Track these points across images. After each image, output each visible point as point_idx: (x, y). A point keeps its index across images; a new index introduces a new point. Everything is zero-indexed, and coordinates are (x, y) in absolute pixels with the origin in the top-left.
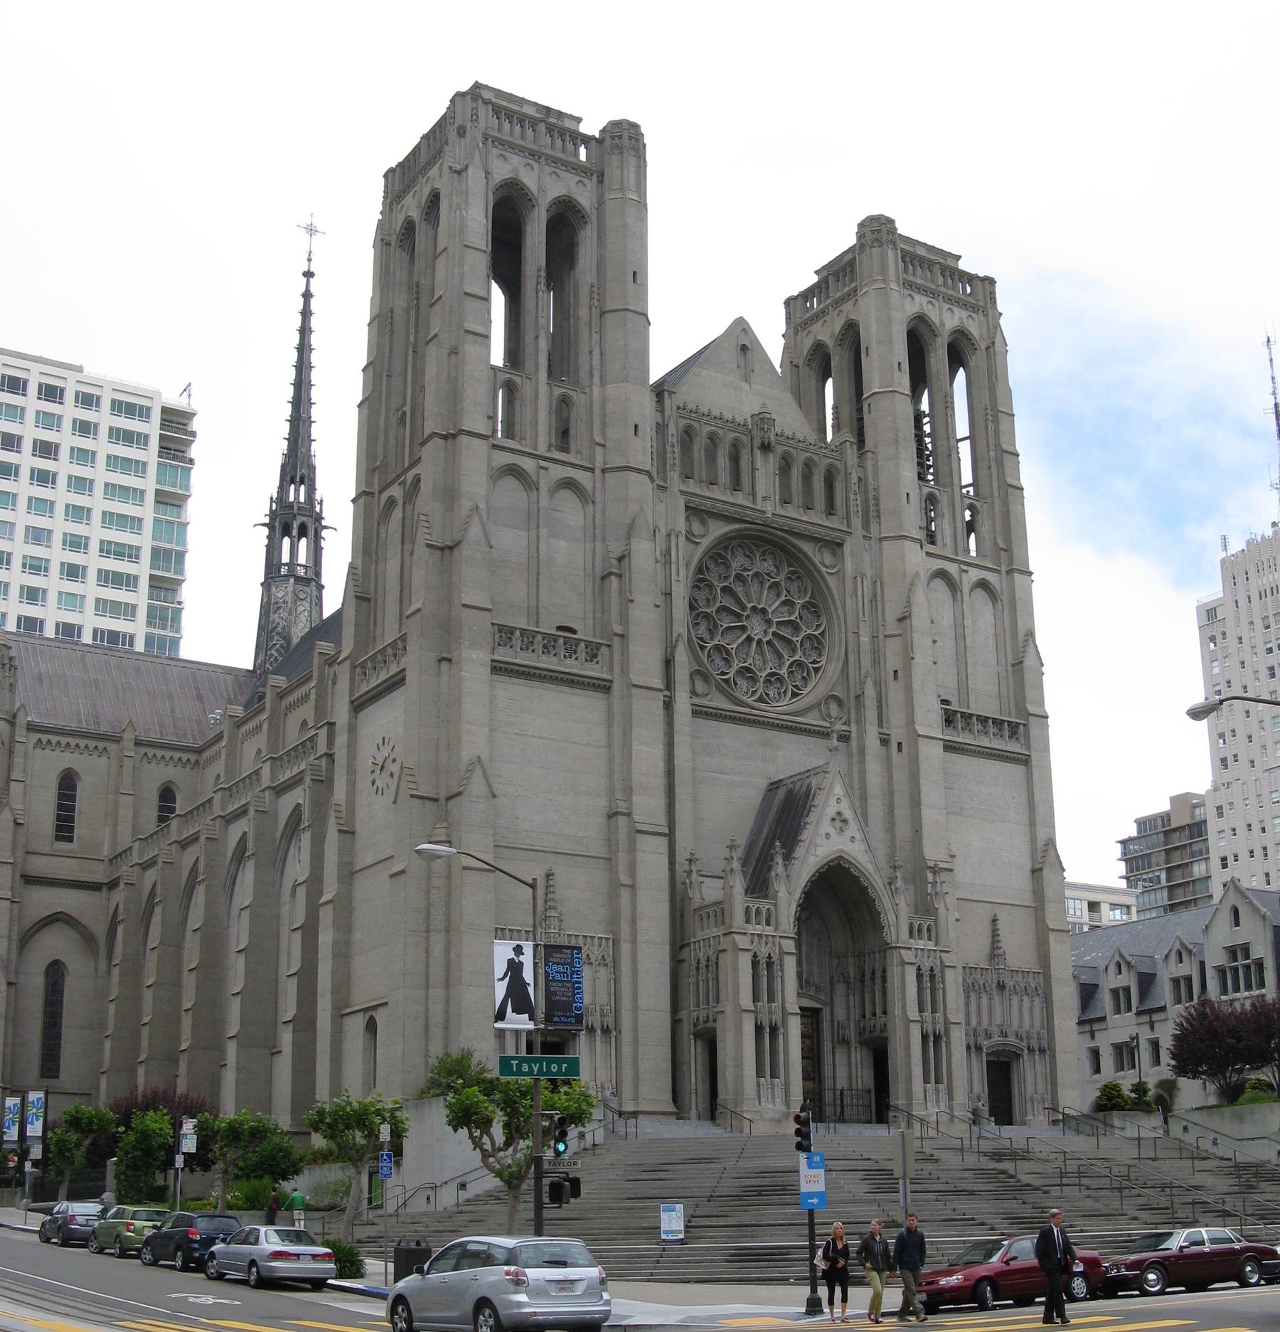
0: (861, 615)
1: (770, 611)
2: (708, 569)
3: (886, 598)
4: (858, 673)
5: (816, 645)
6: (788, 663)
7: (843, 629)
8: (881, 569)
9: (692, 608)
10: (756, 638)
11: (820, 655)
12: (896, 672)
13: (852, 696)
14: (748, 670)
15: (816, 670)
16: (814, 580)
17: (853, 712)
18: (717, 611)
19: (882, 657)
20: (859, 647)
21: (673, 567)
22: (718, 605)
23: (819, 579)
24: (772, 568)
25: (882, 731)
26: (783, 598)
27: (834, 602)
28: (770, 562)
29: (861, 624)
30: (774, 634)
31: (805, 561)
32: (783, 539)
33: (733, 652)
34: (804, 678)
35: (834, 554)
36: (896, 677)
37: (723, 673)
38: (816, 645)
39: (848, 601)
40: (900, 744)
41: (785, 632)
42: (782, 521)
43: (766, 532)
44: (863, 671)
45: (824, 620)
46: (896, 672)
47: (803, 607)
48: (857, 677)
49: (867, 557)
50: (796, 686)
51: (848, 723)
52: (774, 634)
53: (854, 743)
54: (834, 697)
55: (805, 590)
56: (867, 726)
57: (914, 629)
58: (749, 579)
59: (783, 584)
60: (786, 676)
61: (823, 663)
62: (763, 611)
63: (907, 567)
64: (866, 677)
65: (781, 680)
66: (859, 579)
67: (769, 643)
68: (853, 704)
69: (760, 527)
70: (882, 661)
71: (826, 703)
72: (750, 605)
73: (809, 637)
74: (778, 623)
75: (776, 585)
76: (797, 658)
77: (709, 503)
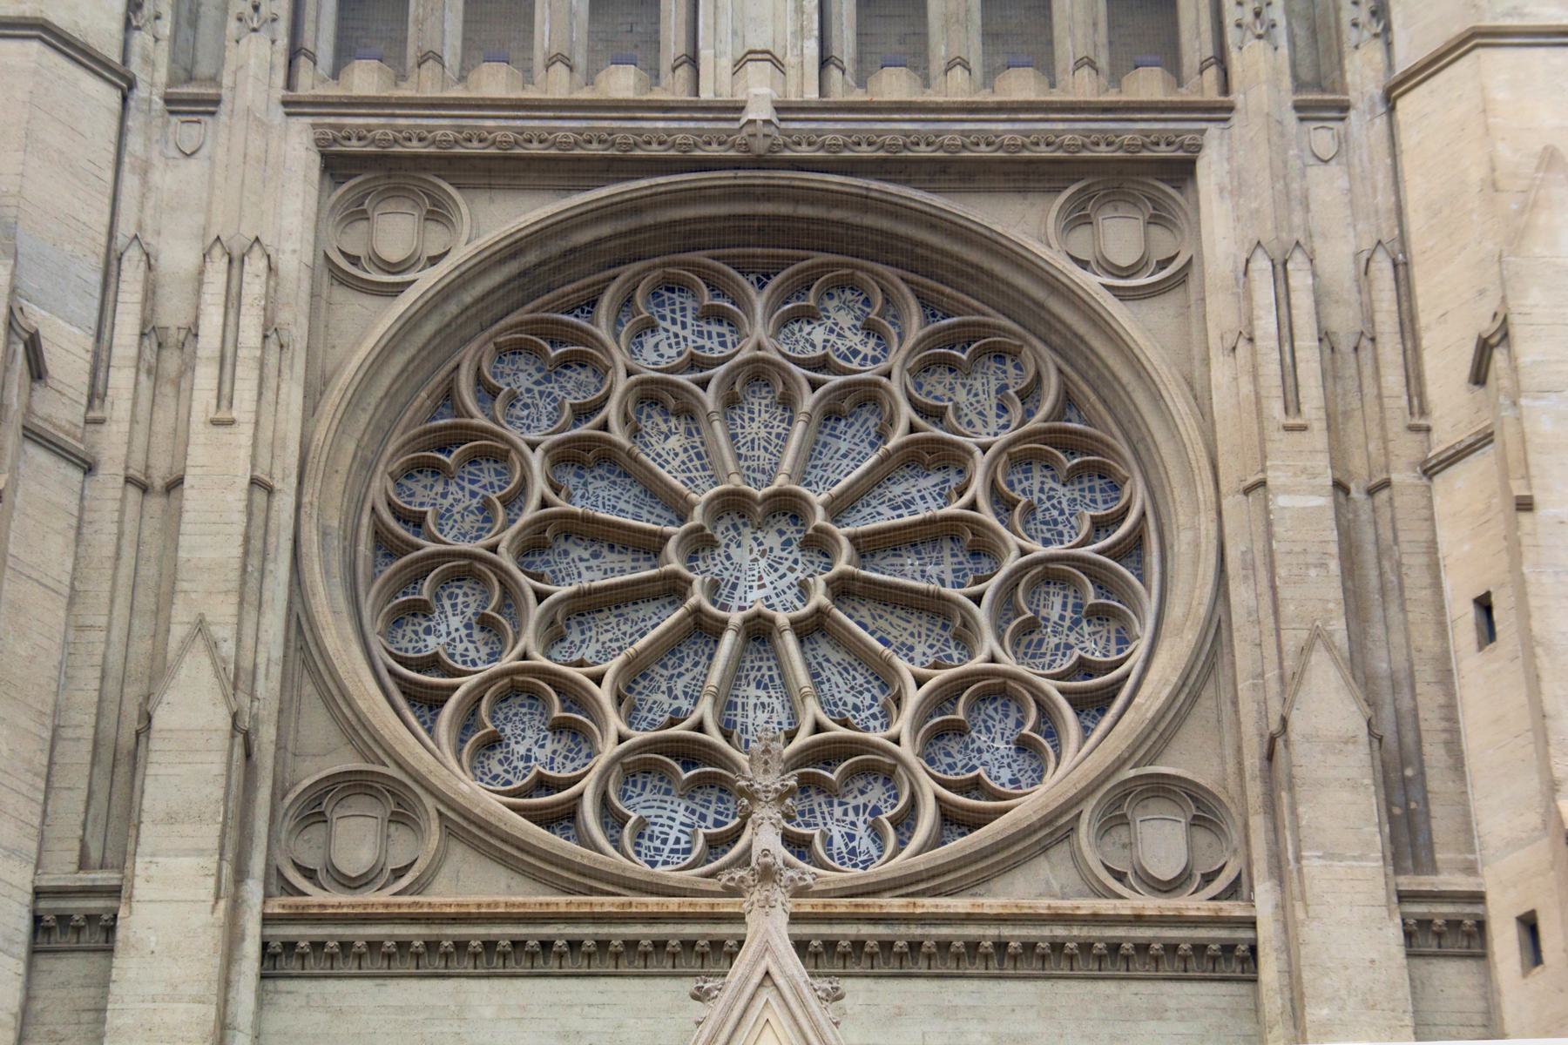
0: (1275, 408)
1: (818, 498)
2: (489, 394)
3: (1424, 319)
4: (1270, 642)
5: (1091, 597)
6: (913, 697)
7: (1205, 492)
8: (1399, 211)
9: (386, 545)
10: (735, 618)
11: (1124, 641)
12: (1484, 605)
13: (1253, 760)
14: (690, 752)
15: (1092, 704)
16: (1069, 348)
17: (1258, 823)
18: (533, 546)
19: (1414, 563)
20: (1269, 535)
21: (205, 377)
22: (530, 512)
23: (1082, 327)
24: (855, 340)
25: (1408, 882)
26: (897, 438)
27: (1157, 397)
28: (845, 320)
29: (1280, 442)
30: (842, 589)
31: (998, 268)
32: (864, 202)
33: (604, 694)
34: (1024, 746)
35: (1160, 218)
36: (1488, 631)
37: (544, 784)
38: (1091, 597)
39: (1221, 372)
40: (1529, 925)
41: (909, 573)
42: (833, 128)
43: (770, 193)
44: (1293, 638)
45: (1137, 494)
46: (1484, 605)
47: (1022, 458)
48: (1272, 674)
49: (1326, 187)
50: (974, 786)
51: (1233, 891)
52: (842, 589)
53: (1270, 968)
54: (1162, 788)
55: (1030, 394)
56: (1313, 864)
57: (1525, 382)
58: (710, 398)
59: (895, 386)
60: (907, 751)
61: (1135, 662)
62: (787, 507)
63: (1504, 152)
64: (1305, 651)
65: (880, 769)
66: (1261, 264)
67: (812, 628)
68: (1255, 790)
69: (724, 177)
70: (1416, 579)
71: (1114, 819)
72: (701, 497)
73: (1049, 575)
74: (869, 546)
75: (867, 397)
76: (977, 663)
77: (442, 125)
